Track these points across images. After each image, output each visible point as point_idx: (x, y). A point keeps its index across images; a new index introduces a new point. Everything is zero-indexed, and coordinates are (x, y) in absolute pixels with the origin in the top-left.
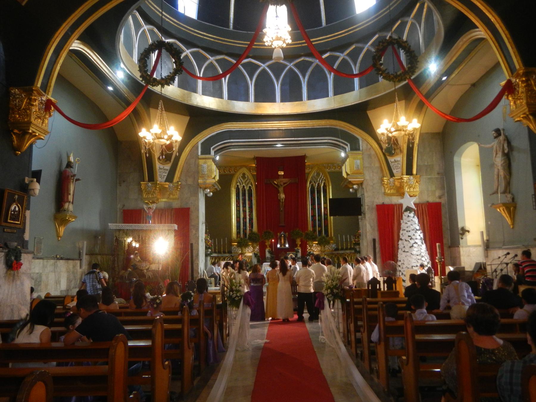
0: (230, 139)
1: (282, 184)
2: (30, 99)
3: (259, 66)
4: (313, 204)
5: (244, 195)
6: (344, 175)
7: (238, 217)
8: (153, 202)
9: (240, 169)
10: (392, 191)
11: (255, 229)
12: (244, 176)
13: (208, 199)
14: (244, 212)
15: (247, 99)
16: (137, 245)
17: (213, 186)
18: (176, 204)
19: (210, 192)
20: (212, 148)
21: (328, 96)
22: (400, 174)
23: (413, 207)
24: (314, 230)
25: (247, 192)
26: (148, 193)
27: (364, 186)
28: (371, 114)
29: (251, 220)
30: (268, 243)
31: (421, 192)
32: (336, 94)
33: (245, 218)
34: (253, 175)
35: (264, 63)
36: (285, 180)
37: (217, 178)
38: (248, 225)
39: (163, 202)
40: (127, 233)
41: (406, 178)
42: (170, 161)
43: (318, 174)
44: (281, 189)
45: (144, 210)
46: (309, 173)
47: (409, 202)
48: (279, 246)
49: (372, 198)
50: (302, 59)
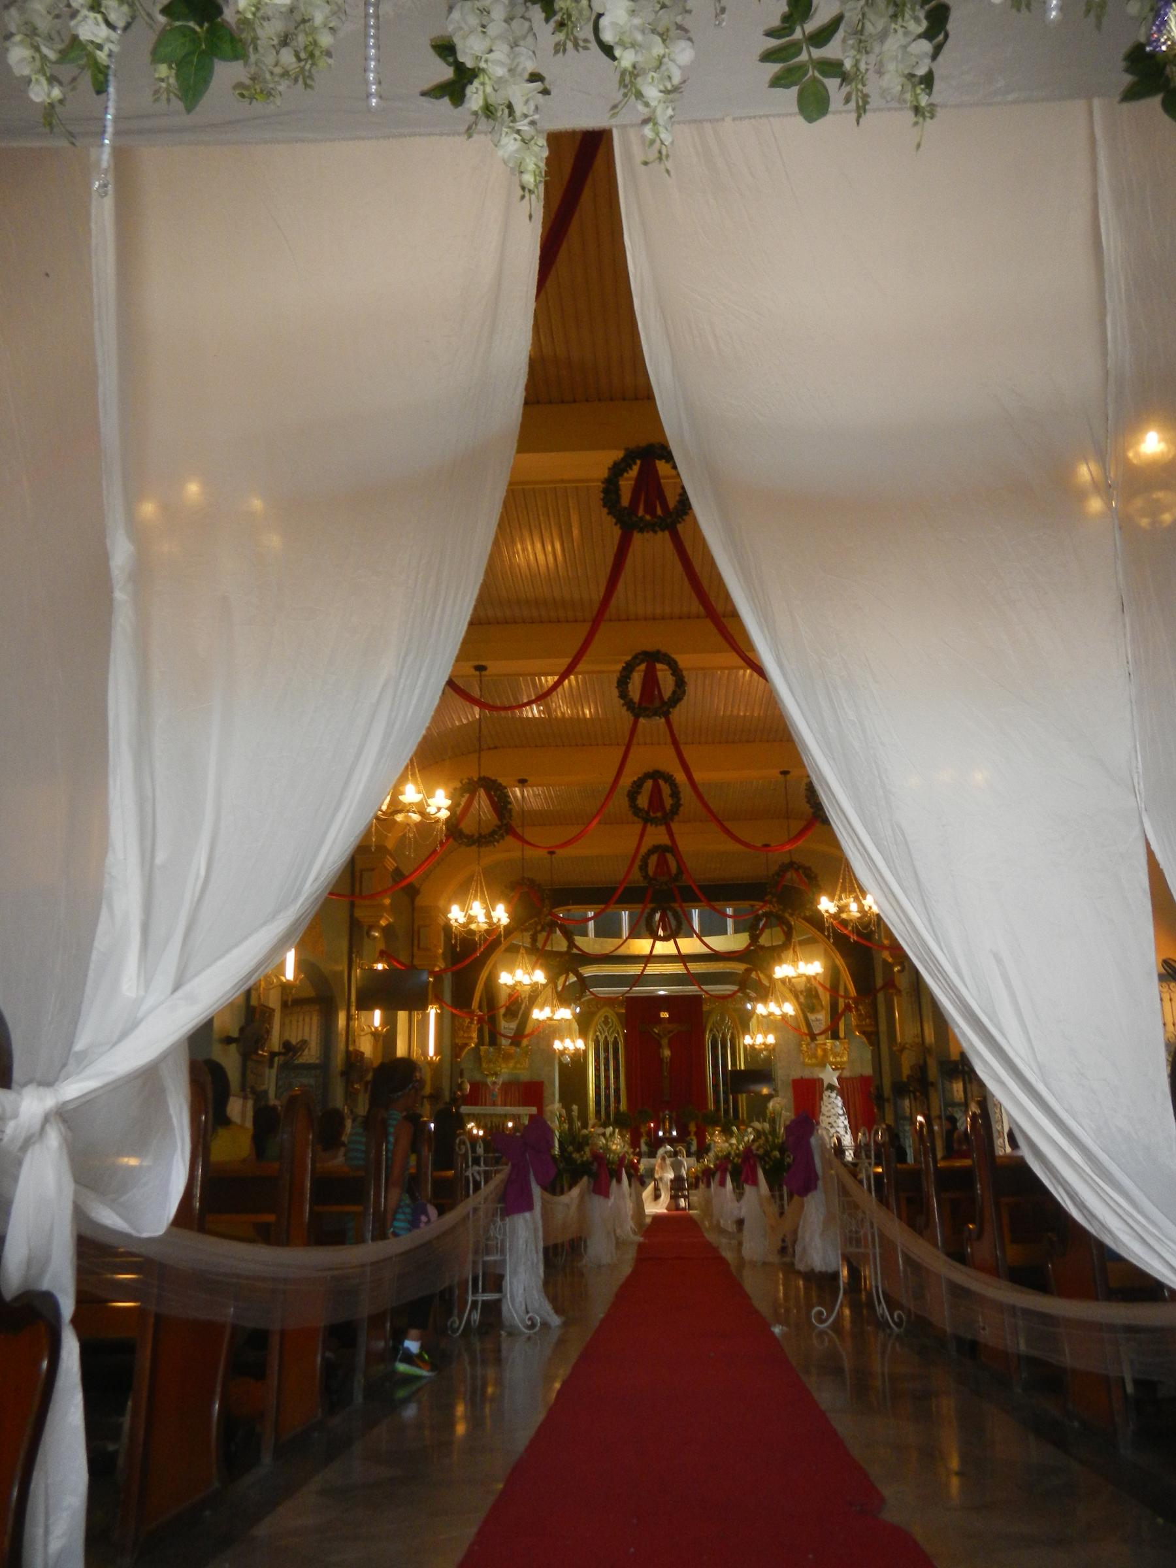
2: (472, 1019)
4: (715, 1066)
5: (606, 1050)
7: (598, 1087)
8: (496, 1074)
9: (599, 1009)
10: (814, 1061)
11: (623, 1106)
12: (606, 1022)
13: (560, 1062)
14: (607, 1078)
16: (481, 1133)
18: (525, 1076)
21: (726, 933)
23: (836, 1083)
24: (718, 1109)
25: (611, 1046)
26: (490, 1061)
29: (617, 1090)
30: (643, 1130)
31: (850, 1061)
32: (736, 931)
33: (607, 1087)
34: (618, 1014)
38: (612, 1099)
39: (506, 1071)
40: (475, 1118)
43: (723, 1019)
44: (665, 1042)
45: (486, 1084)
46: (710, 1013)
47: (830, 1076)
48: (661, 1134)
49: (785, 1072)
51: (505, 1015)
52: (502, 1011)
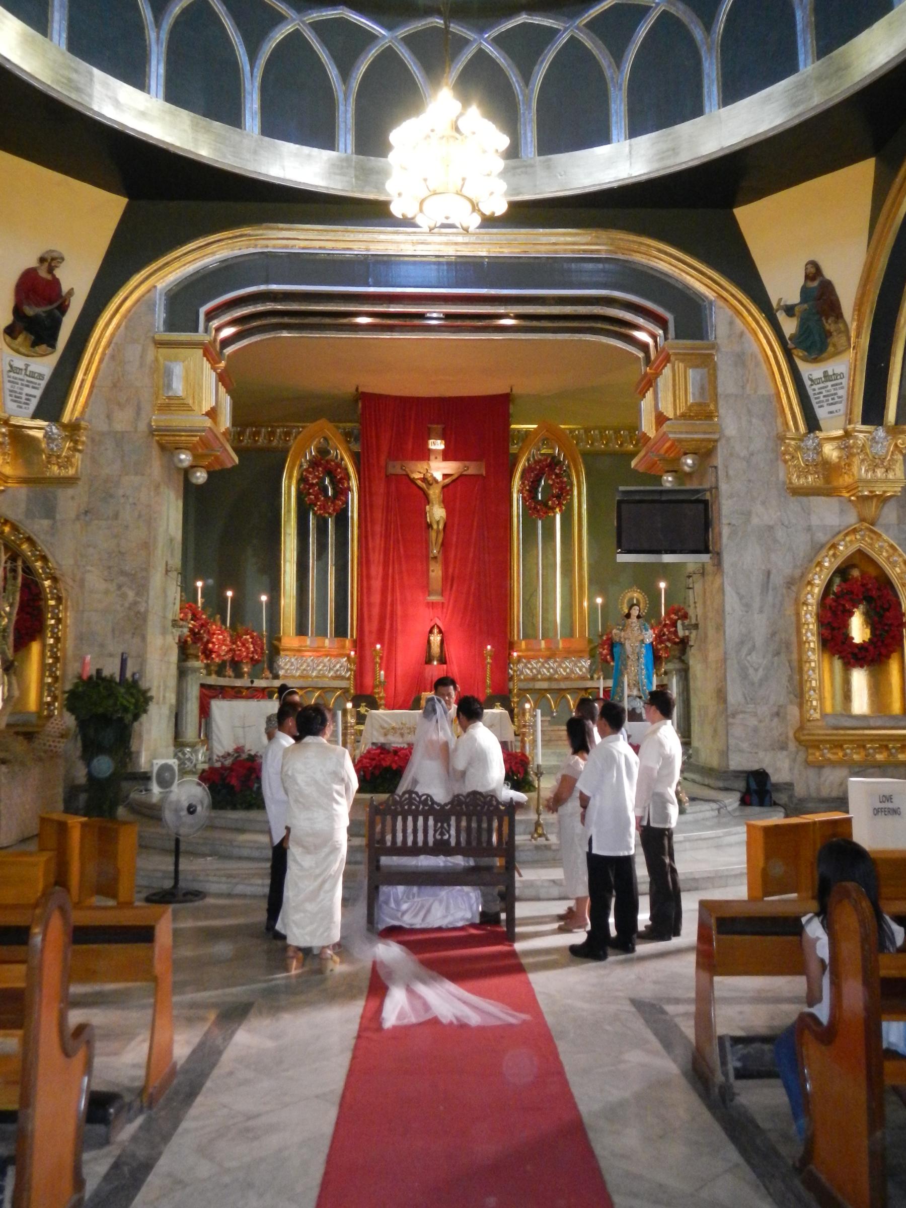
0: (267, 282)
1: (439, 477)
3: (372, 38)
6: (648, 426)
15: (327, 141)
17: (204, 442)
20: (203, 310)
22: (842, 420)
27: (719, 460)
28: (751, 218)
35: (390, 27)
36: (451, 467)
37: (226, 421)
41: (862, 432)
42: (52, 345)
44: (435, 493)
50: (523, 18)
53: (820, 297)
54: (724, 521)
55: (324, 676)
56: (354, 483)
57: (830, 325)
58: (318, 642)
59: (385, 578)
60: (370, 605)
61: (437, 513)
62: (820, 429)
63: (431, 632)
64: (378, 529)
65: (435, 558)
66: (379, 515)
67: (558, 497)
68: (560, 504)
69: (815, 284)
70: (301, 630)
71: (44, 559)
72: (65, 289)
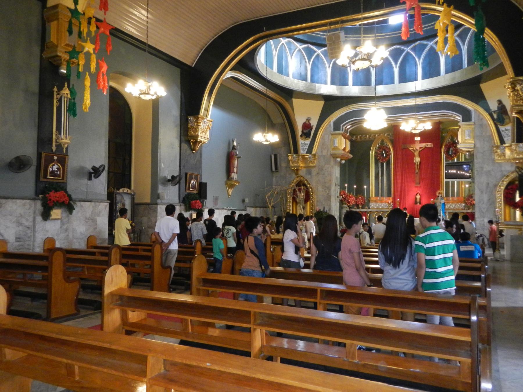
1: (418, 148)
2: (198, 122)
19: (341, 160)
20: (341, 126)
26: (293, 163)
28: (484, 86)
36: (423, 145)
42: (310, 137)
44: (416, 153)
50: (418, 42)
51: (301, 136)
52: (300, 133)
53: (502, 109)
54: (475, 170)
55: (383, 208)
56: (392, 152)
57: (504, 116)
58: (382, 198)
59: (402, 179)
60: (397, 187)
61: (417, 160)
62: (505, 144)
63: (417, 195)
64: (399, 165)
65: (417, 173)
66: (399, 161)
67: (455, 154)
68: (456, 156)
69: (500, 106)
70: (377, 195)
71: (309, 184)
72: (312, 125)
